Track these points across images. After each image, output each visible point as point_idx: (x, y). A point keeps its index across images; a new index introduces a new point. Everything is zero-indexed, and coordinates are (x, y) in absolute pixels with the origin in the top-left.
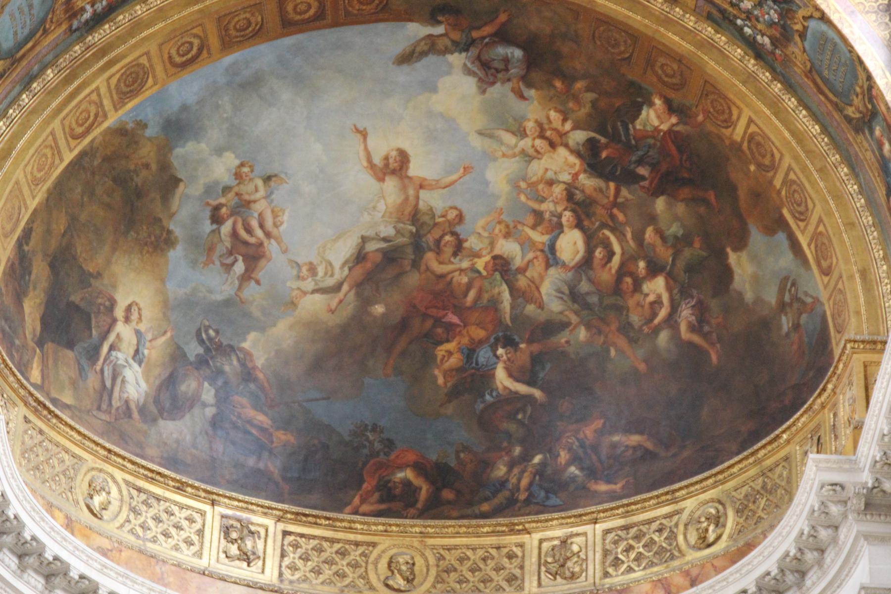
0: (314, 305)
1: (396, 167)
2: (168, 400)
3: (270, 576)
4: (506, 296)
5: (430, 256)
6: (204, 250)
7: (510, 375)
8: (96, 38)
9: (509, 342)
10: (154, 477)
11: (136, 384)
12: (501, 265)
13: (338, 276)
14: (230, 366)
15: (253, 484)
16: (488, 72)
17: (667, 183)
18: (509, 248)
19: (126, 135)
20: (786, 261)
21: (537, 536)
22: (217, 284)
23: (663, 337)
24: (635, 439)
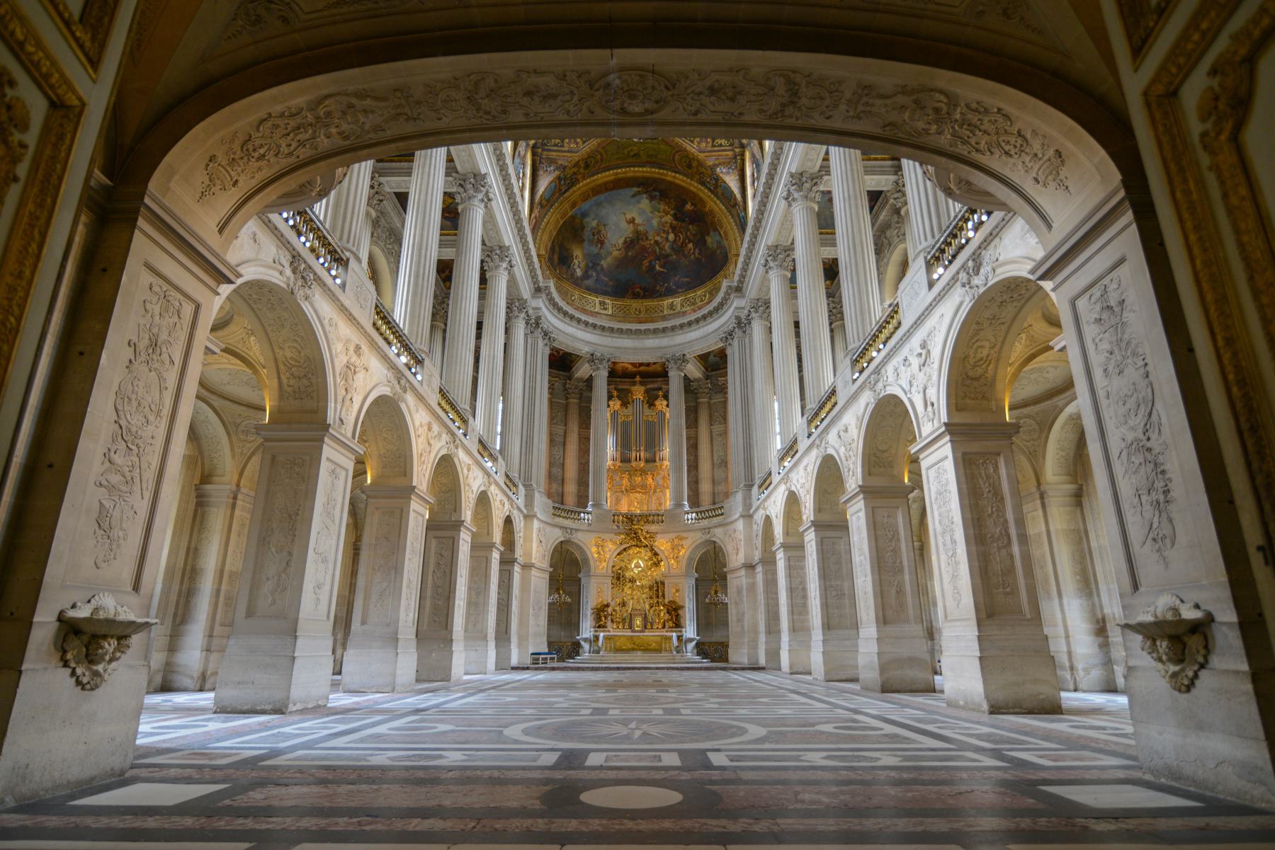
0: (616, 253)
1: (632, 221)
2: (586, 276)
6: (591, 242)
11: (579, 273)
12: (656, 242)
15: (605, 293)
16: (652, 198)
17: (692, 222)
18: (658, 238)
19: (573, 217)
20: (718, 238)
22: (595, 250)
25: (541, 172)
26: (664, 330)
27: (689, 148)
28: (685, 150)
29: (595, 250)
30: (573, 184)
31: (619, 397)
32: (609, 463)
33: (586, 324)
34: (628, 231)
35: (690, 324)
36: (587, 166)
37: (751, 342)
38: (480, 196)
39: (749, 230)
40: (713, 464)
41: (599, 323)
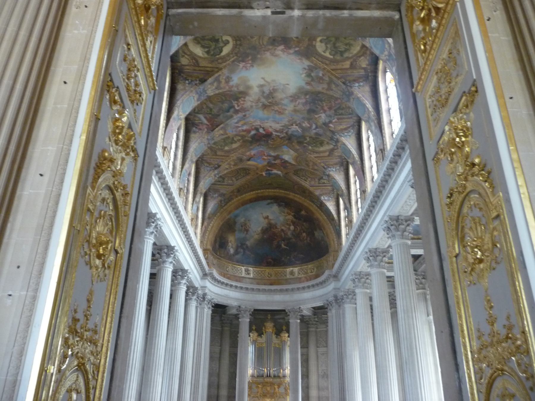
0: (256, 237)
1: (267, 217)
2: (236, 252)
3: (252, 276)
4: (283, 235)
5: (272, 230)
7: (285, 245)
8: (224, 208)
9: (284, 241)
10: (235, 264)
12: (282, 230)
13: (260, 232)
14: (245, 247)
16: (279, 206)
18: (283, 228)
19: (229, 219)
21: (288, 270)
22: (242, 235)
23: (305, 241)
24: (302, 256)
25: (209, 198)
26: (287, 290)
27: (303, 184)
28: (301, 185)
29: (242, 235)
30: (230, 201)
31: (257, 330)
32: (248, 378)
33: (236, 287)
34: (264, 223)
35: (304, 288)
36: (239, 191)
37: (344, 314)
38: (170, 260)
39: (342, 254)
40: (318, 375)
41: (244, 286)
